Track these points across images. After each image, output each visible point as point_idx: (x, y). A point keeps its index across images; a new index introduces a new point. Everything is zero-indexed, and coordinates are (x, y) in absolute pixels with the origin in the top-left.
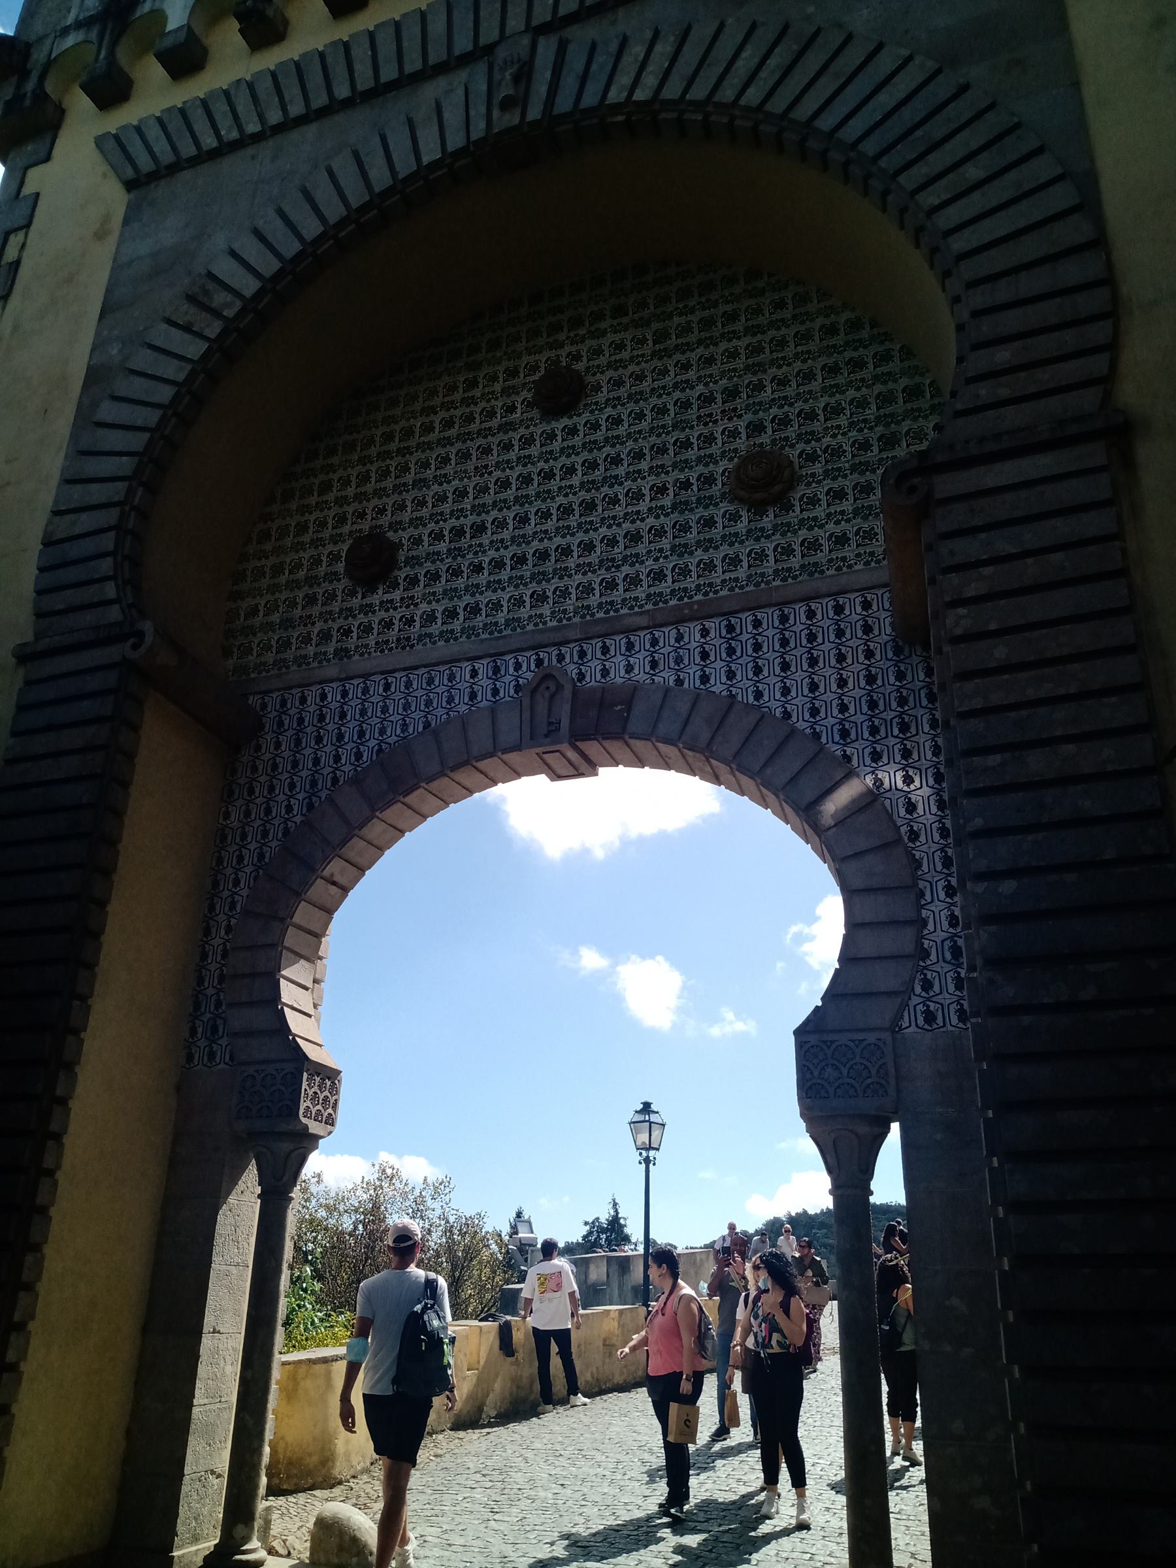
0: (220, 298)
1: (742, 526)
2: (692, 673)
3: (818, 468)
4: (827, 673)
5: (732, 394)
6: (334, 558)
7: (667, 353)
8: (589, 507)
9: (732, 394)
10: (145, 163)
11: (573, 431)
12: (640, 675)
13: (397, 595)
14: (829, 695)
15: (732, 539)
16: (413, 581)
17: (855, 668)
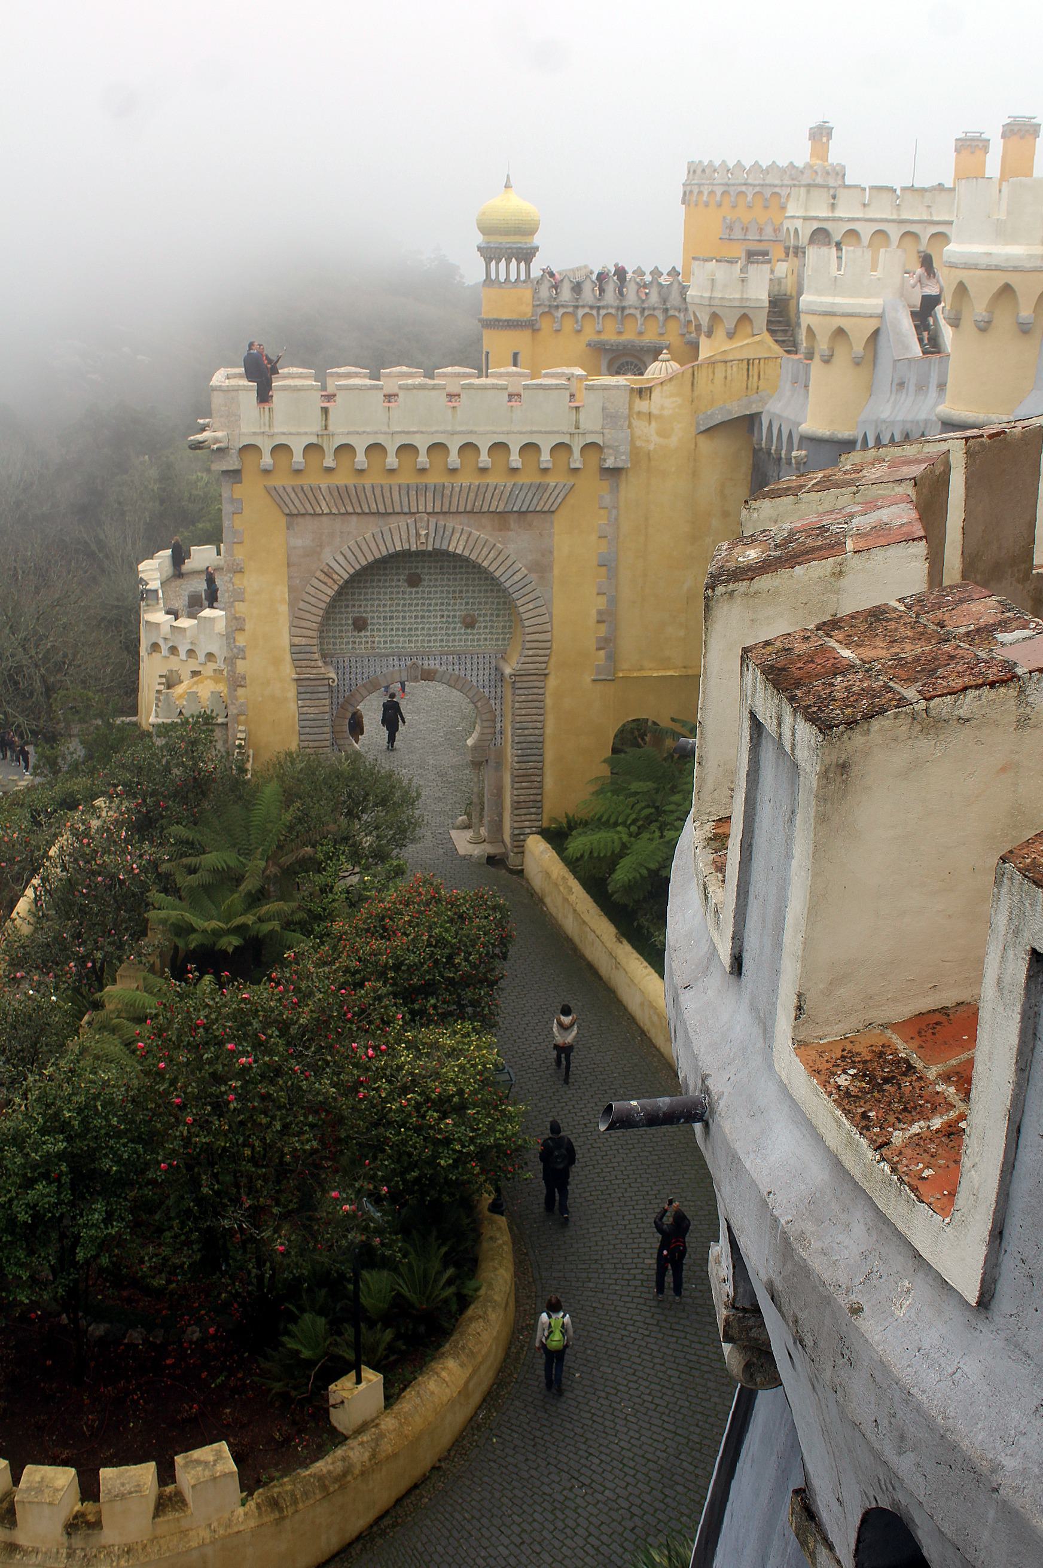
0: (335, 577)
1: (463, 631)
2: (450, 667)
3: (482, 619)
4: (481, 672)
5: (461, 592)
6: (347, 618)
7: (443, 574)
8: (423, 617)
9: (461, 592)
10: (296, 512)
11: (417, 593)
12: (438, 666)
13: (368, 634)
14: (481, 678)
15: (460, 634)
16: (372, 630)
17: (487, 672)
